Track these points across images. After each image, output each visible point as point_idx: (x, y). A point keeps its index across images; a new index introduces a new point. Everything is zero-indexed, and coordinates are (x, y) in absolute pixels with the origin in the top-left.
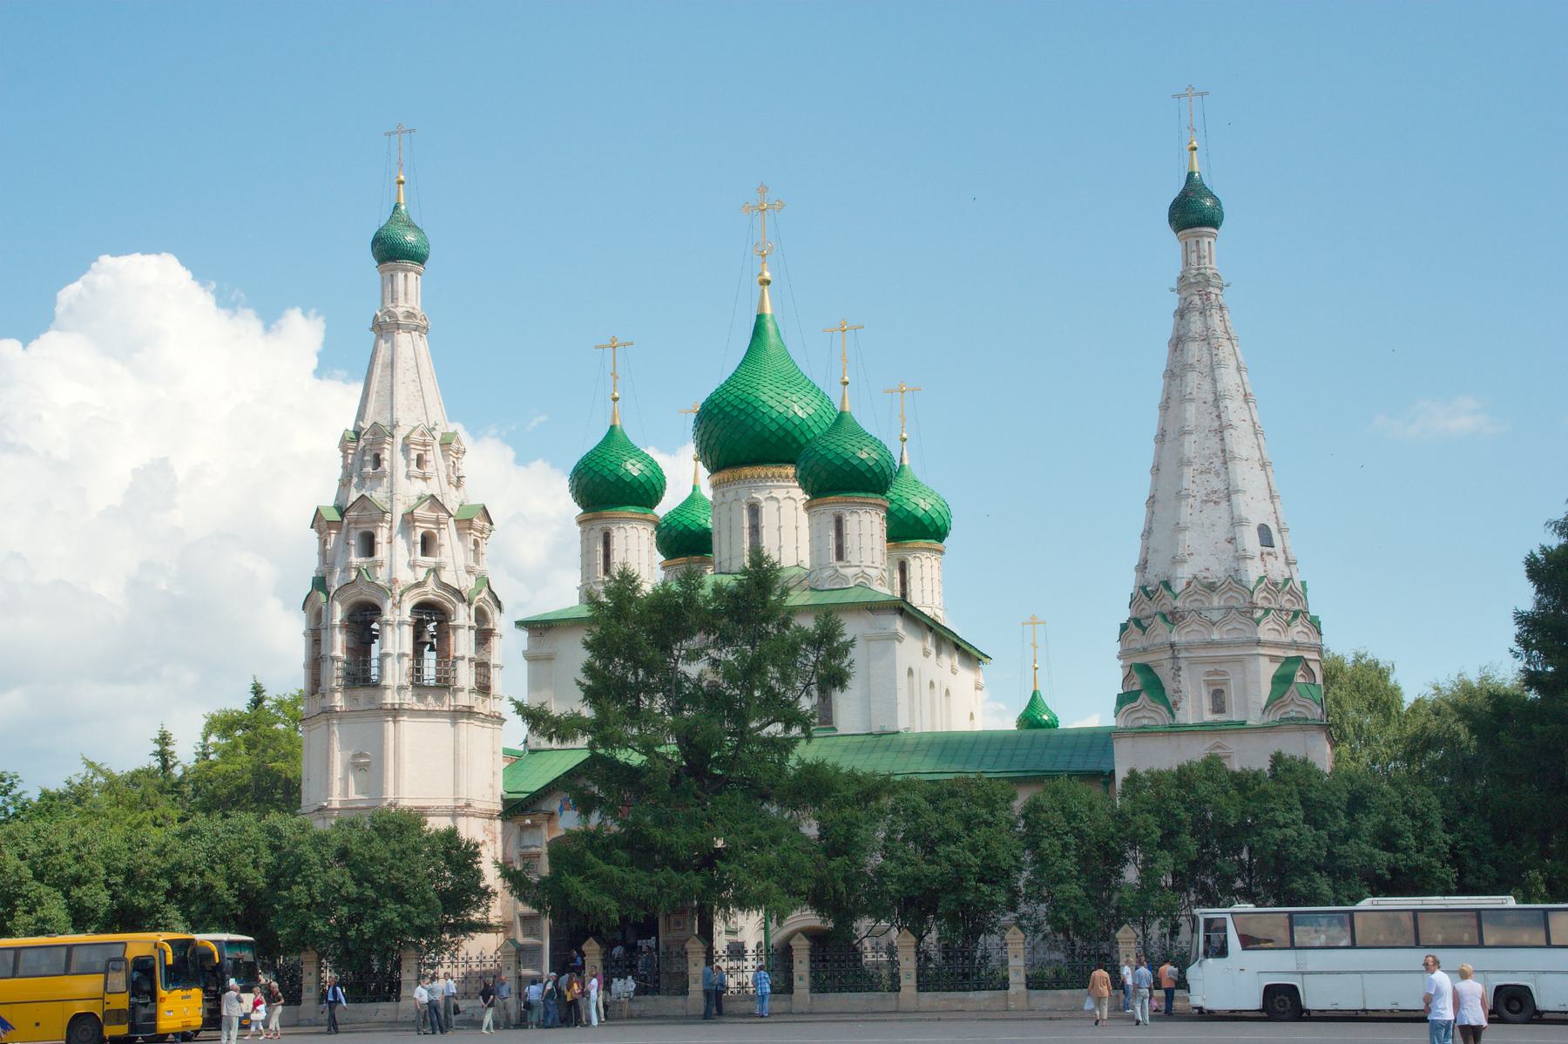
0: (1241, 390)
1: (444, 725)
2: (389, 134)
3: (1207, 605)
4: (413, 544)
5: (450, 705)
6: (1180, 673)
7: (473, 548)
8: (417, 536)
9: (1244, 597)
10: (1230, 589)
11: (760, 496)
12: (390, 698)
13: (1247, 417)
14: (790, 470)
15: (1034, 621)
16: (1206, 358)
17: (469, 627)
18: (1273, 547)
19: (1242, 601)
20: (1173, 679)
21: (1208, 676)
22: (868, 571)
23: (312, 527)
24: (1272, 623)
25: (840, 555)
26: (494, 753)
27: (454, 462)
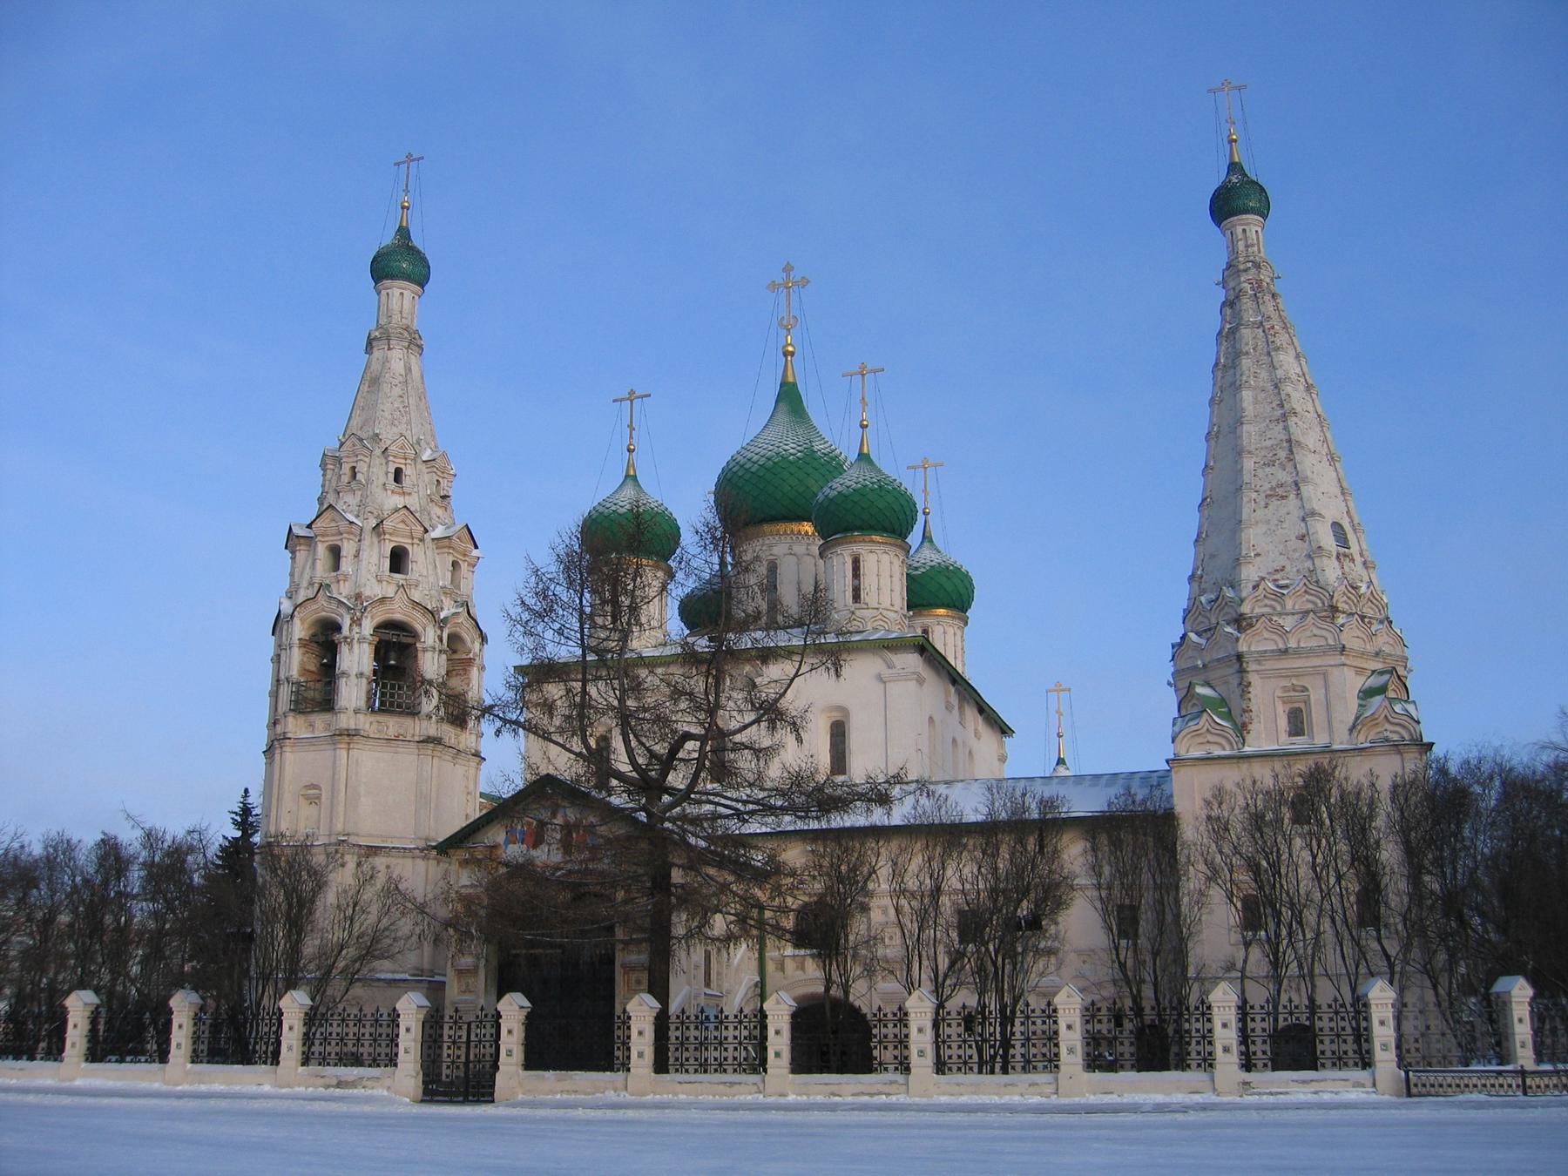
0: (1302, 380)
1: (408, 761)
2: (398, 164)
3: (1279, 608)
4: (381, 556)
5: (413, 736)
6: (1251, 689)
7: (451, 568)
8: (388, 548)
9: (1321, 599)
10: (1306, 592)
11: (779, 549)
12: (345, 721)
13: (1311, 409)
14: (808, 527)
15: (1058, 689)
16: (1261, 344)
17: (440, 651)
18: (1349, 548)
19: (1320, 605)
20: (1241, 696)
21: (1285, 692)
22: (885, 613)
23: (286, 548)
24: (1356, 629)
25: (856, 597)
26: (468, 793)
27: (438, 481)
